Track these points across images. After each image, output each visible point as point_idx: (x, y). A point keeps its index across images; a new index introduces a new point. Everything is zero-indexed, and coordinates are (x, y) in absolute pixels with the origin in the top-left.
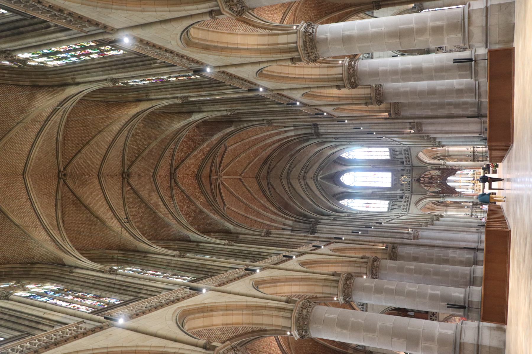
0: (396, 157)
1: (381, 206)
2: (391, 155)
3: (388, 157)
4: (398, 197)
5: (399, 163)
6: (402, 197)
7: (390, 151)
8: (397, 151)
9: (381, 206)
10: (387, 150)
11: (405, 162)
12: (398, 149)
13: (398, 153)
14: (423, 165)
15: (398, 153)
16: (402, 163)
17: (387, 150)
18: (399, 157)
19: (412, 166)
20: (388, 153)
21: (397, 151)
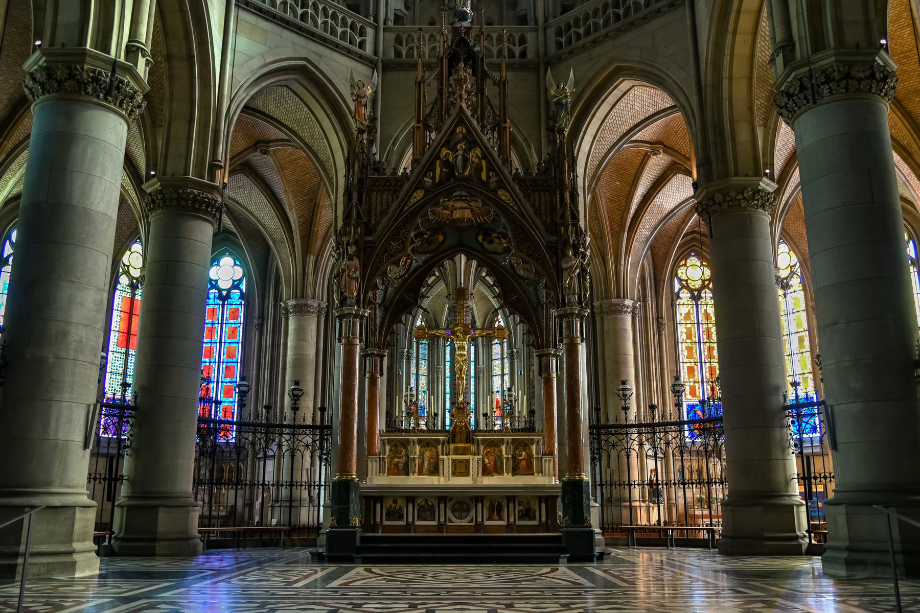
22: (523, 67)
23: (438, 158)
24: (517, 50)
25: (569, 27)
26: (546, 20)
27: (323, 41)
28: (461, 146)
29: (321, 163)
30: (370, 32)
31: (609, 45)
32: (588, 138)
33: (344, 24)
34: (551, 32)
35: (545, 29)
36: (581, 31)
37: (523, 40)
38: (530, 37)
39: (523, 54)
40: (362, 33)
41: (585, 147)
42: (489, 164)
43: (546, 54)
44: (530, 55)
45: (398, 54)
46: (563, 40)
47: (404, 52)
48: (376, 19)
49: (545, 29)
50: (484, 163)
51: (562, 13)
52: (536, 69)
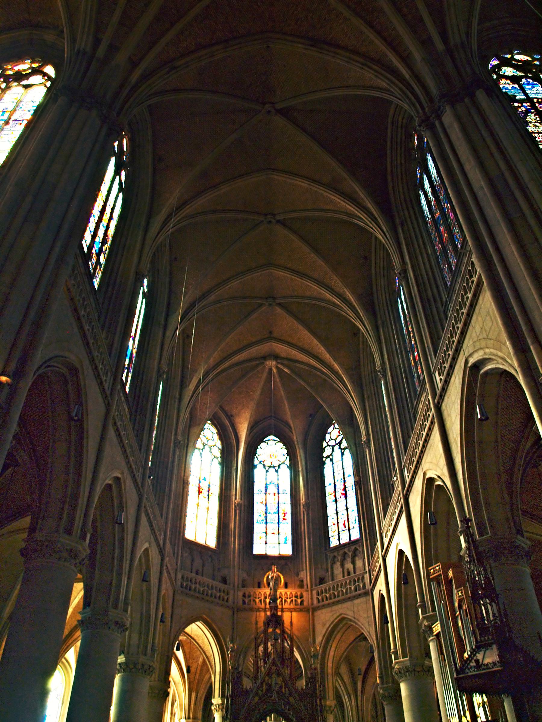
0: (338, 564)
1: (201, 524)
2: (341, 546)
3: (334, 543)
4: (225, 572)
5: (321, 573)
6: (224, 581)
7: (351, 543)
8: (353, 563)
9: (201, 524)
10: (356, 535)
11: (323, 587)
12: (359, 563)
13: (349, 566)
14: (319, 639)
15: (349, 566)
16: (322, 581)
17: (356, 535)
18: (338, 570)
19: (315, 609)
20: (345, 539)
21: (353, 563)
22: (301, 610)
23: (264, 681)
24: (299, 601)
25: (322, 593)
26: (311, 587)
27: (212, 602)
28: (274, 676)
29: (207, 657)
30: (231, 592)
31: (340, 606)
32: (333, 649)
33: (220, 591)
34: (314, 592)
35: (311, 591)
36: (328, 596)
37: (301, 597)
38: (304, 594)
39: (302, 602)
40: (228, 594)
41: (332, 653)
42: (285, 684)
43: (312, 604)
44: (305, 604)
45: (244, 602)
46: (320, 598)
47: (247, 600)
48: (234, 586)
49: (311, 591)
50: (283, 684)
51: (320, 584)
52: (308, 611)
